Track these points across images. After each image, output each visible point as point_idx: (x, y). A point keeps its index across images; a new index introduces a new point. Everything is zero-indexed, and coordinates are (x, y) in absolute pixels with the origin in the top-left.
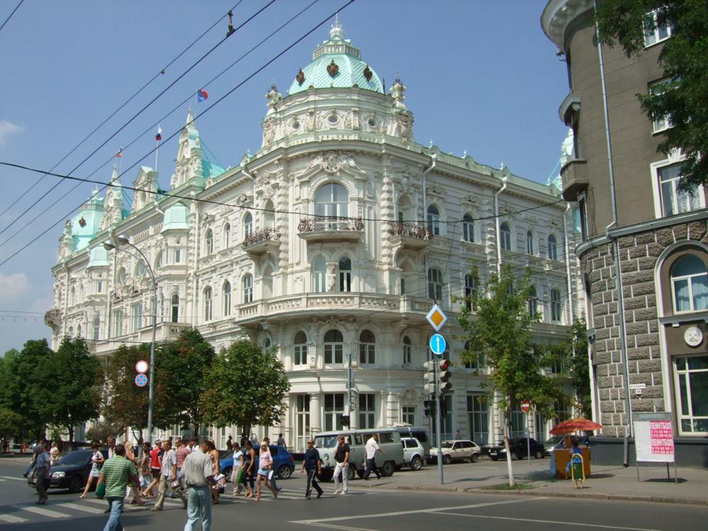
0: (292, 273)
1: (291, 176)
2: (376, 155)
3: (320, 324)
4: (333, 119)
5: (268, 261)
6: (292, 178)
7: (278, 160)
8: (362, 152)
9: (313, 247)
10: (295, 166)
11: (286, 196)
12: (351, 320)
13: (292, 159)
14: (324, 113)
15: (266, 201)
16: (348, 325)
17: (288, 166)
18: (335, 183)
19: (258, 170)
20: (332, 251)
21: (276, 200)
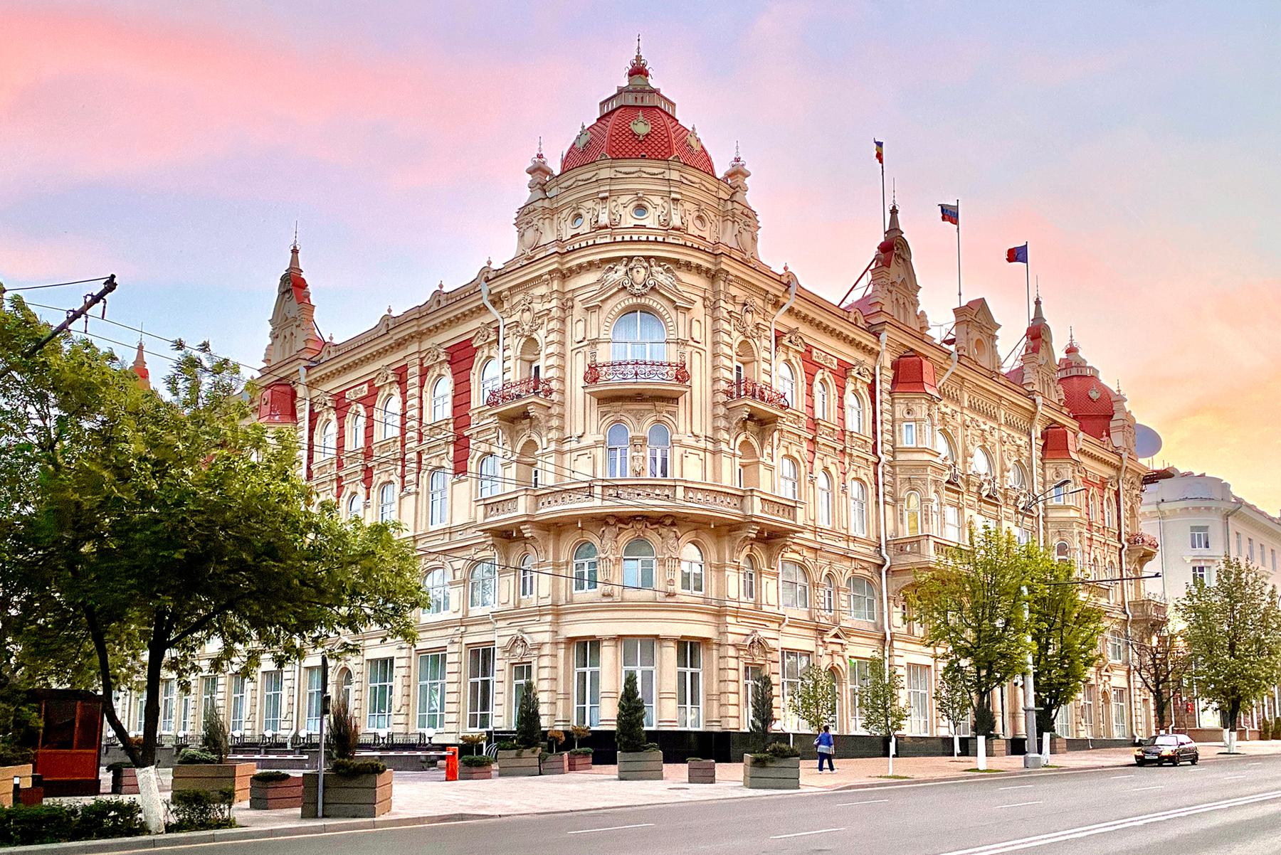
0: (571, 451)
1: (567, 300)
2: (708, 270)
3: (620, 528)
4: (641, 209)
5: (528, 432)
6: (570, 304)
7: (550, 273)
8: (688, 265)
9: (606, 409)
10: (574, 283)
11: (562, 332)
12: (668, 521)
13: (570, 270)
14: (624, 199)
15: (524, 340)
16: (664, 531)
17: (564, 282)
18: (647, 310)
19: (510, 289)
20: (639, 417)
21: (540, 335)
